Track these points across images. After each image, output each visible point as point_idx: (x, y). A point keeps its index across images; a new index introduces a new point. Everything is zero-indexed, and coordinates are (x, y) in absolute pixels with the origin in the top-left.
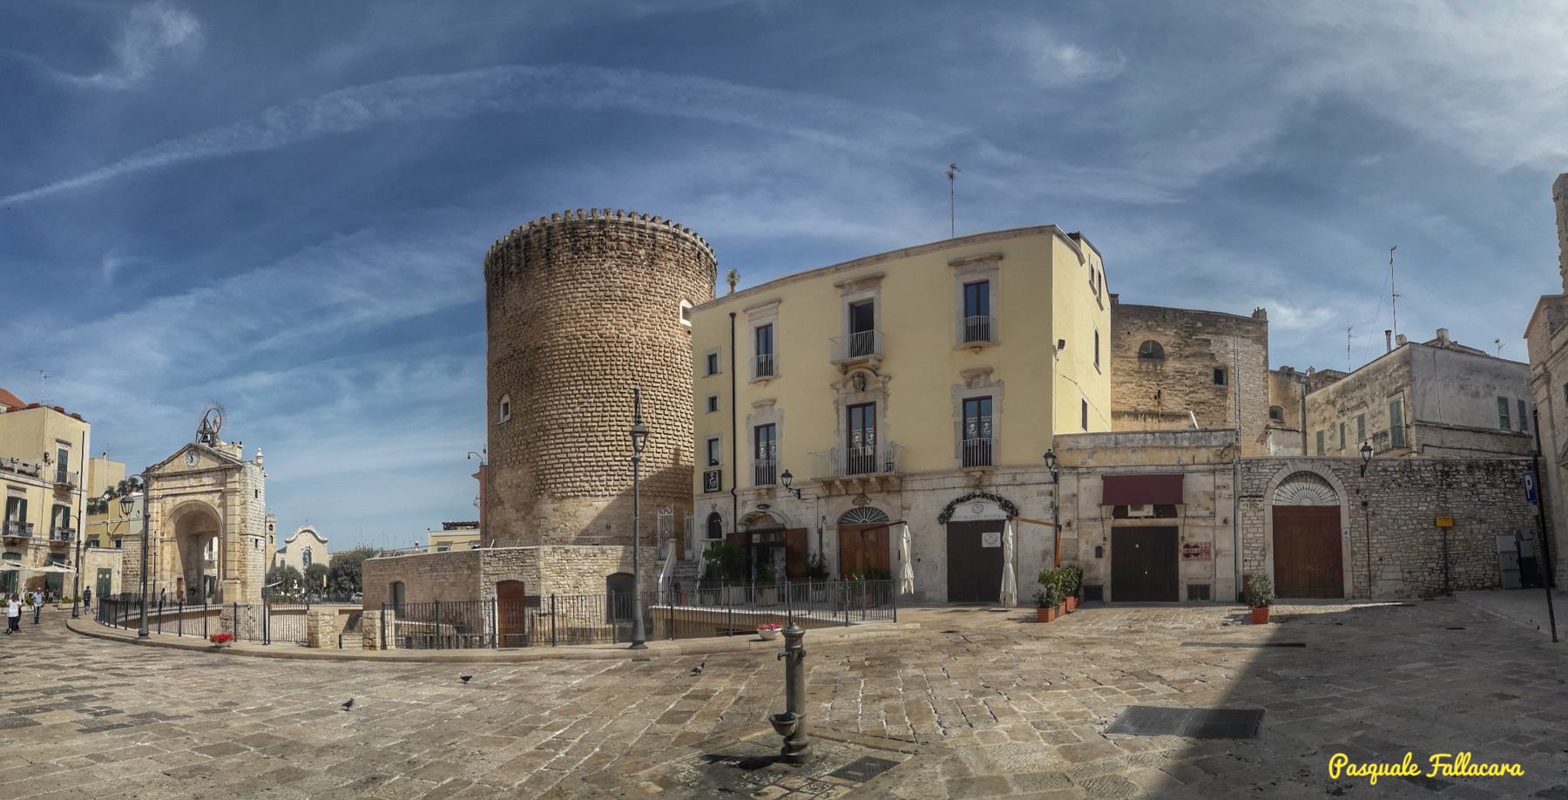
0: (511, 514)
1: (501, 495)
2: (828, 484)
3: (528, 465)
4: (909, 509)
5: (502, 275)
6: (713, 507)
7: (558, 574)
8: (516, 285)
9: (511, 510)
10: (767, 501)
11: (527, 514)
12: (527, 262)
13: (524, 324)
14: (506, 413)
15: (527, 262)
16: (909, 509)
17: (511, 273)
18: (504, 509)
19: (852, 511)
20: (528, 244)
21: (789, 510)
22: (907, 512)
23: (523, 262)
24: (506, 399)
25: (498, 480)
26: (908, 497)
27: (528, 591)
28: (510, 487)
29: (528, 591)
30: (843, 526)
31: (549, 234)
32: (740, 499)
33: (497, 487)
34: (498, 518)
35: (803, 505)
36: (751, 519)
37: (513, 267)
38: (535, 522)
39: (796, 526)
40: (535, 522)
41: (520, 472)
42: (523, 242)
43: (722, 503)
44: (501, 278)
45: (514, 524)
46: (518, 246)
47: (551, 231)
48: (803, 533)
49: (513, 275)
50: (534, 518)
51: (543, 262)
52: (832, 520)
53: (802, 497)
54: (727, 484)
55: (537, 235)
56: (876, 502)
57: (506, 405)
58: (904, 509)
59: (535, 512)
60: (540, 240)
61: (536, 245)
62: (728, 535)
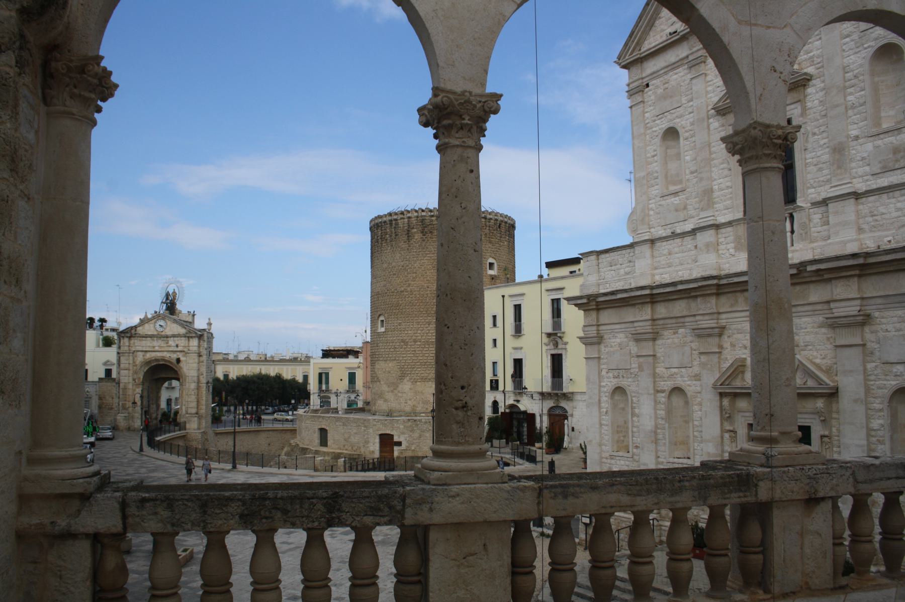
0: (385, 388)
1: (379, 376)
2: (542, 394)
3: (395, 362)
4: (576, 408)
5: (381, 238)
6: (495, 398)
7: (411, 431)
8: (389, 248)
9: (384, 386)
10: (519, 399)
11: (394, 389)
12: (396, 235)
13: (394, 274)
14: (382, 326)
15: (396, 235)
16: (576, 408)
17: (386, 240)
18: (381, 384)
19: (554, 407)
20: (397, 224)
21: (527, 405)
22: (575, 409)
23: (394, 235)
24: (382, 318)
25: (377, 366)
26: (575, 403)
27: (396, 439)
28: (384, 372)
29: (396, 439)
30: (551, 414)
31: (409, 221)
32: (507, 395)
33: (376, 370)
34: (377, 389)
35: (534, 402)
36: (512, 406)
37: (388, 236)
38: (400, 394)
39: (531, 412)
40: (400, 394)
41: (390, 365)
42: (394, 222)
43: (499, 397)
44: (380, 240)
45: (387, 394)
46: (391, 224)
47: (410, 220)
48: (533, 416)
49: (388, 241)
50: (399, 392)
51: (405, 238)
52: (545, 411)
53: (534, 398)
54: (501, 388)
55: (402, 220)
56: (563, 404)
57: (382, 321)
58: (574, 408)
59: (400, 389)
60: (404, 224)
61: (401, 226)
62: (502, 413)
